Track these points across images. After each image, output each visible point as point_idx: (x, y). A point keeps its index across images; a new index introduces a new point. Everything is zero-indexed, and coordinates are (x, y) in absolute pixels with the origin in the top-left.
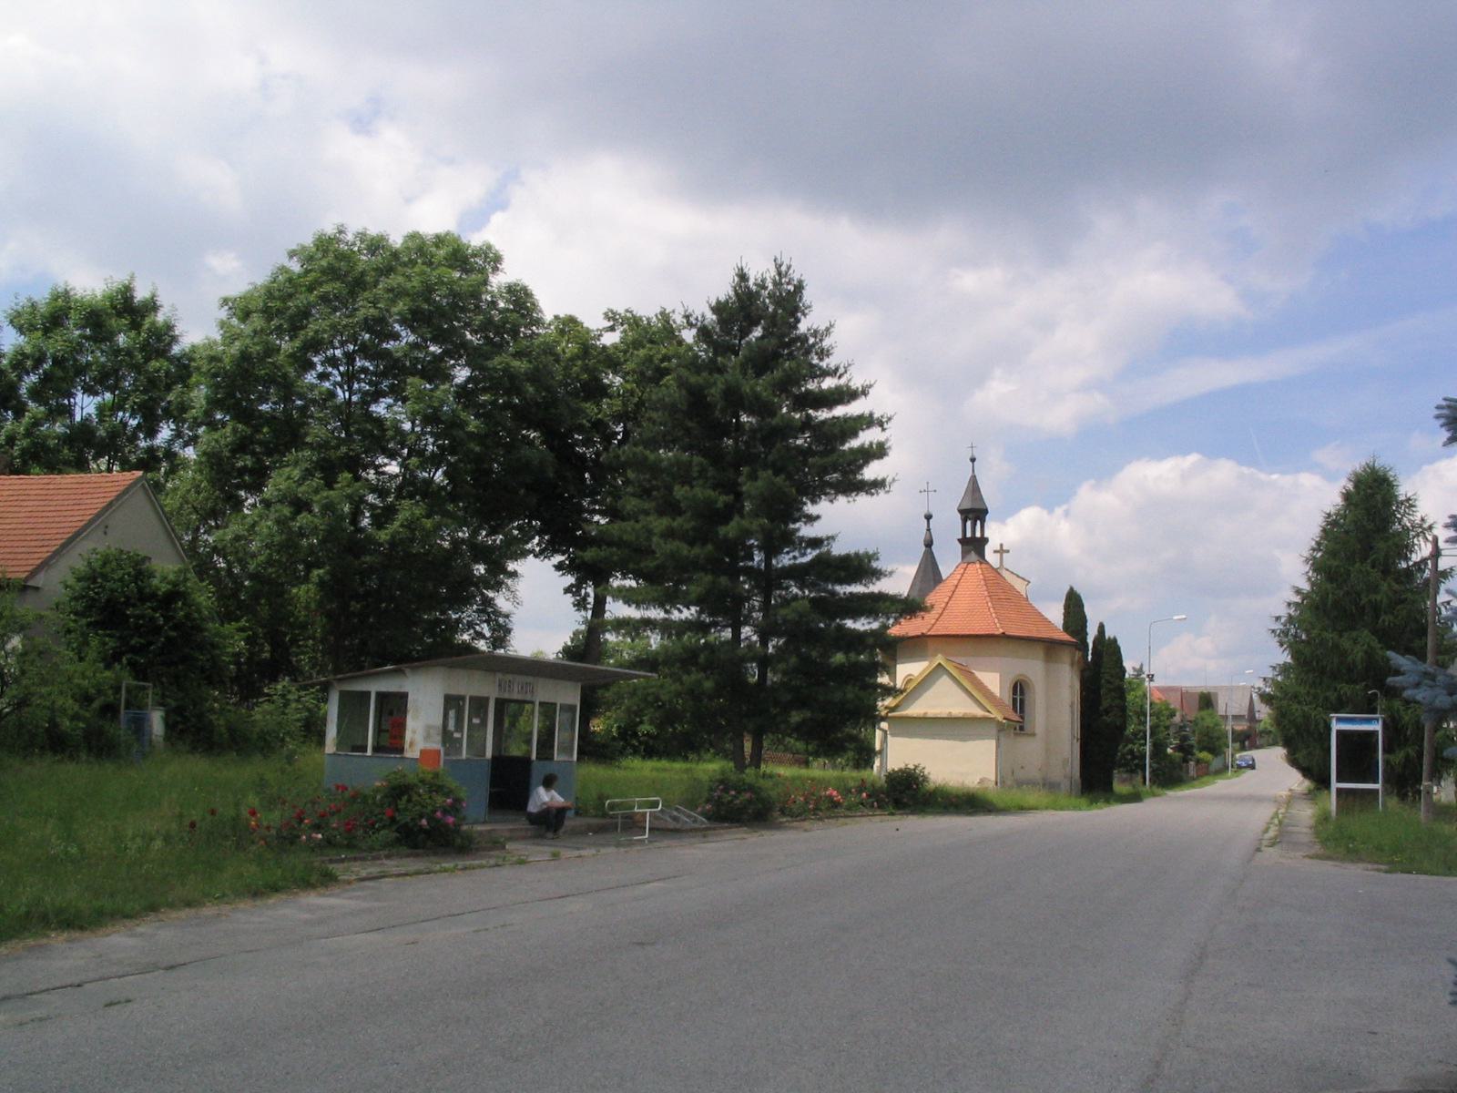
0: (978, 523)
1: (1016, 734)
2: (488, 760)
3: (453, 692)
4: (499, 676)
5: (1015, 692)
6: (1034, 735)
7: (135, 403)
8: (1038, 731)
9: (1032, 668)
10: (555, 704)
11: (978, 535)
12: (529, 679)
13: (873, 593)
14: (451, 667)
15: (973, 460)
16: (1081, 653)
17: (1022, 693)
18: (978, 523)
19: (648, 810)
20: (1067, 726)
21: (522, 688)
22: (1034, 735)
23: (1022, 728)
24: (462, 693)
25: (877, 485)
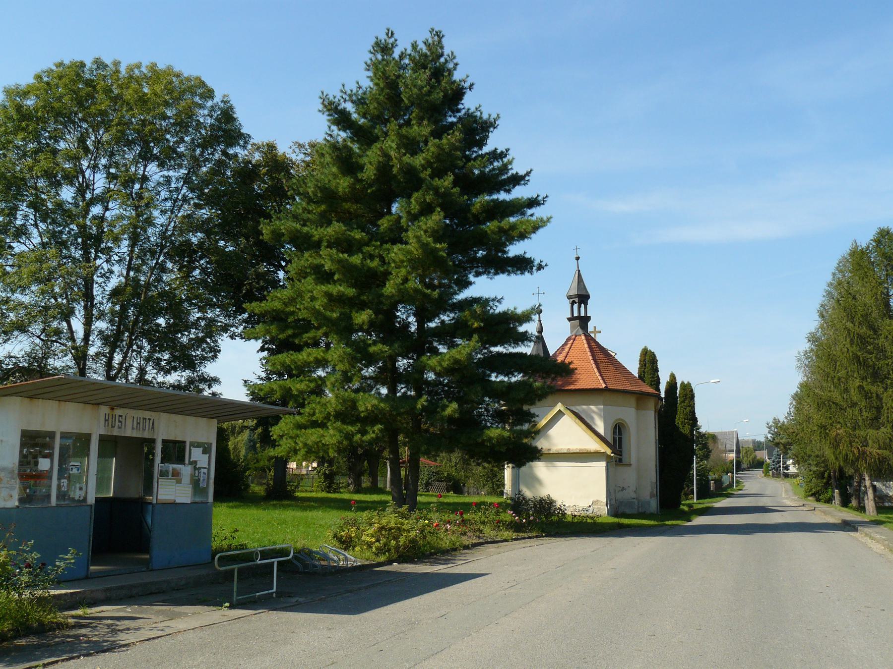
0: (583, 305)
1: (616, 465)
2: (91, 506)
3: (35, 426)
4: (105, 410)
5: (614, 433)
6: (630, 465)
7: (97, 84)
8: (633, 461)
9: (628, 413)
10: (184, 442)
11: (583, 314)
12: (147, 414)
13: (522, 353)
14: (31, 397)
15: (578, 259)
16: (263, 493)
17: (620, 433)
18: (583, 305)
19: (275, 560)
20: (653, 458)
21: (138, 423)
22: (630, 465)
23: (620, 460)
24: (48, 427)
25: (523, 265)
